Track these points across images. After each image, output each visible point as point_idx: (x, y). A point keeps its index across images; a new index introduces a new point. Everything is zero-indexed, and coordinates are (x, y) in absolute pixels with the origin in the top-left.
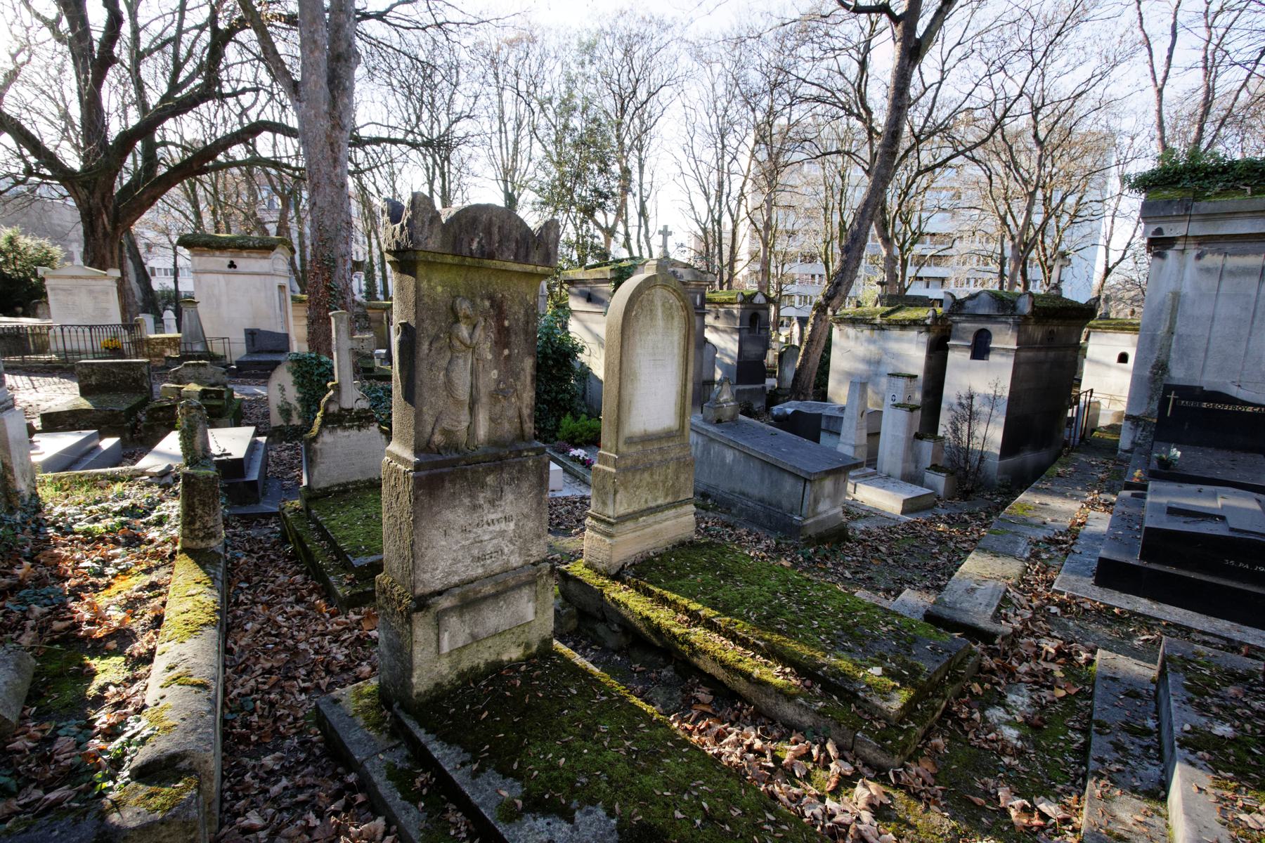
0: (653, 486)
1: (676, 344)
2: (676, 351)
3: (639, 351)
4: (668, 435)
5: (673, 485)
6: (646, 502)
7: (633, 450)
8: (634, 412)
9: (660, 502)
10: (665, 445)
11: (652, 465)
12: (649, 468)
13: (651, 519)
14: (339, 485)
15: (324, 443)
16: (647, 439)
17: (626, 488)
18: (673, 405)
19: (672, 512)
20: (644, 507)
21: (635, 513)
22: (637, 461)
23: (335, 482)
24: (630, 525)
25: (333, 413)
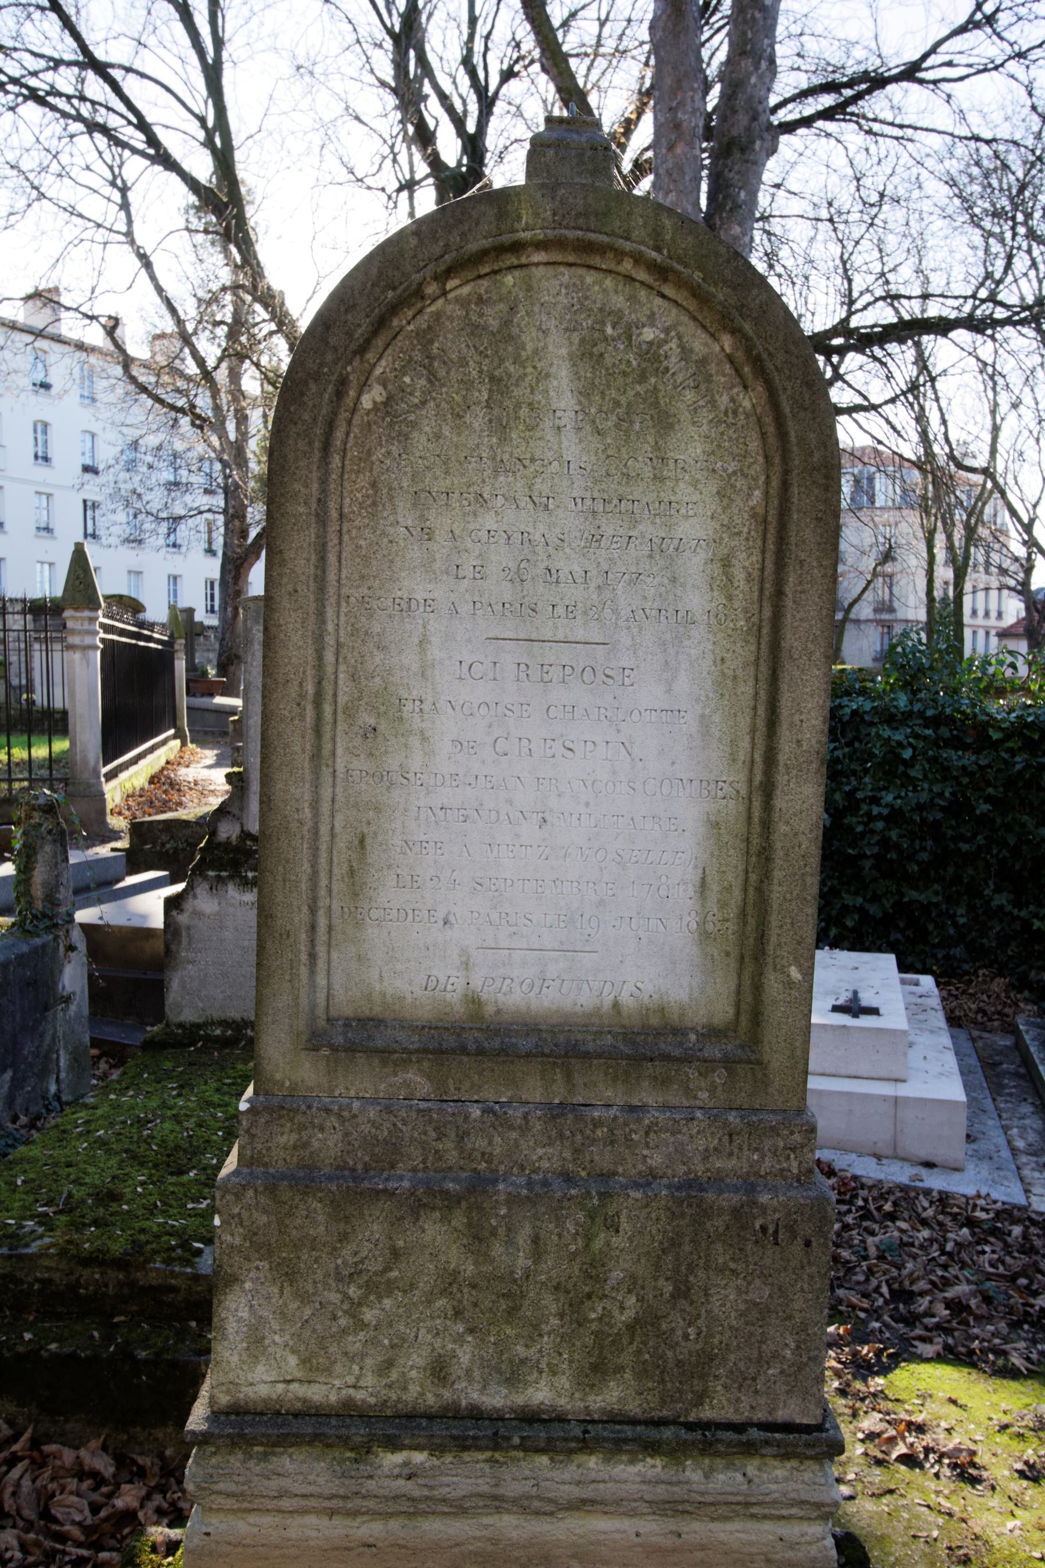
0: (492, 1303)
1: (695, 565)
2: (697, 599)
3: (415, 586)
4: (639, 1046)
5: (645, 1323)
6: (439, 1370)
7: (362, 1084)
8: (388, 894)
9: (540, 1394)
10: (604, 1094)
11: (480, 1185)
12: (466, 1195)
13: (466, 1475)
14: (224, 1023)
15: (197, 914)
16: (475, 1044)
17: (288, 1274)
18: (683, 899)
19: (635, 1474)
20: (418, 1391)
21: (349, 1413)
22: (388, 1154)
23: (217, 1015)
24: (303, 1471)
25: (228, 842)
